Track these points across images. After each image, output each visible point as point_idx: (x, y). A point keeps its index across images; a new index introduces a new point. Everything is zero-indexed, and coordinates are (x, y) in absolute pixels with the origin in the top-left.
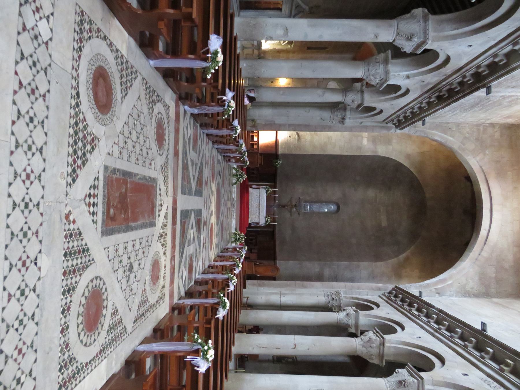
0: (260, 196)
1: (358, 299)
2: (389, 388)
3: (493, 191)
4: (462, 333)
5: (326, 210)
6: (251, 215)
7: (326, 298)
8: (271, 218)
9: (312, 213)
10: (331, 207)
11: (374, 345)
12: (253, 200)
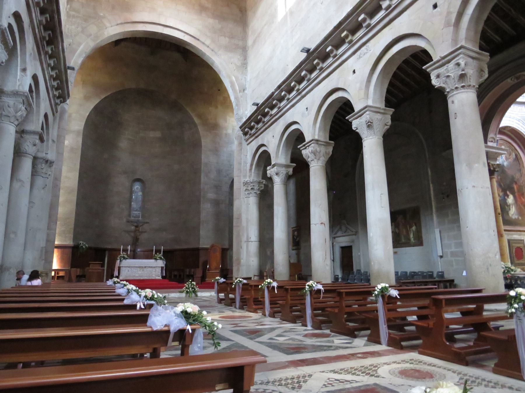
0: (129, 267)
1: (251, 165)
2: (373, 136)
4: (307, 70)
6: (153, 277)
7: (251, 195)
8: (156, 253)
9: (143, 208)
11: (318, 149)
12: (134, 274)
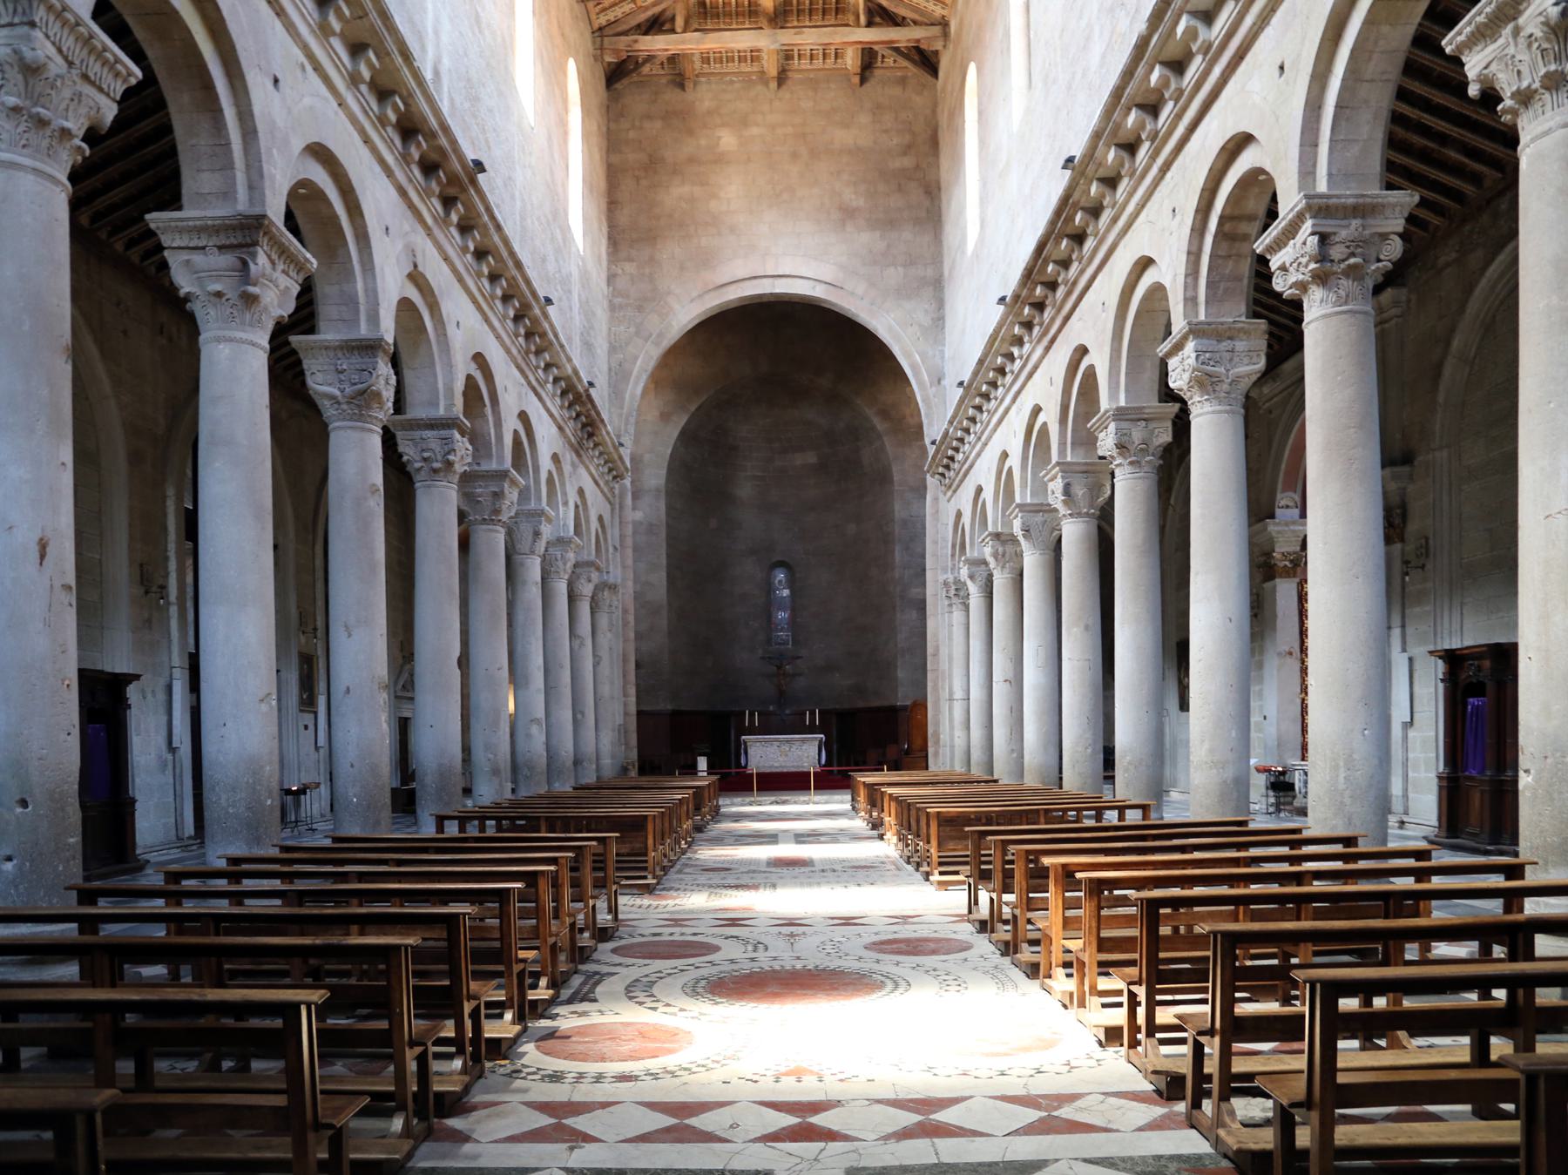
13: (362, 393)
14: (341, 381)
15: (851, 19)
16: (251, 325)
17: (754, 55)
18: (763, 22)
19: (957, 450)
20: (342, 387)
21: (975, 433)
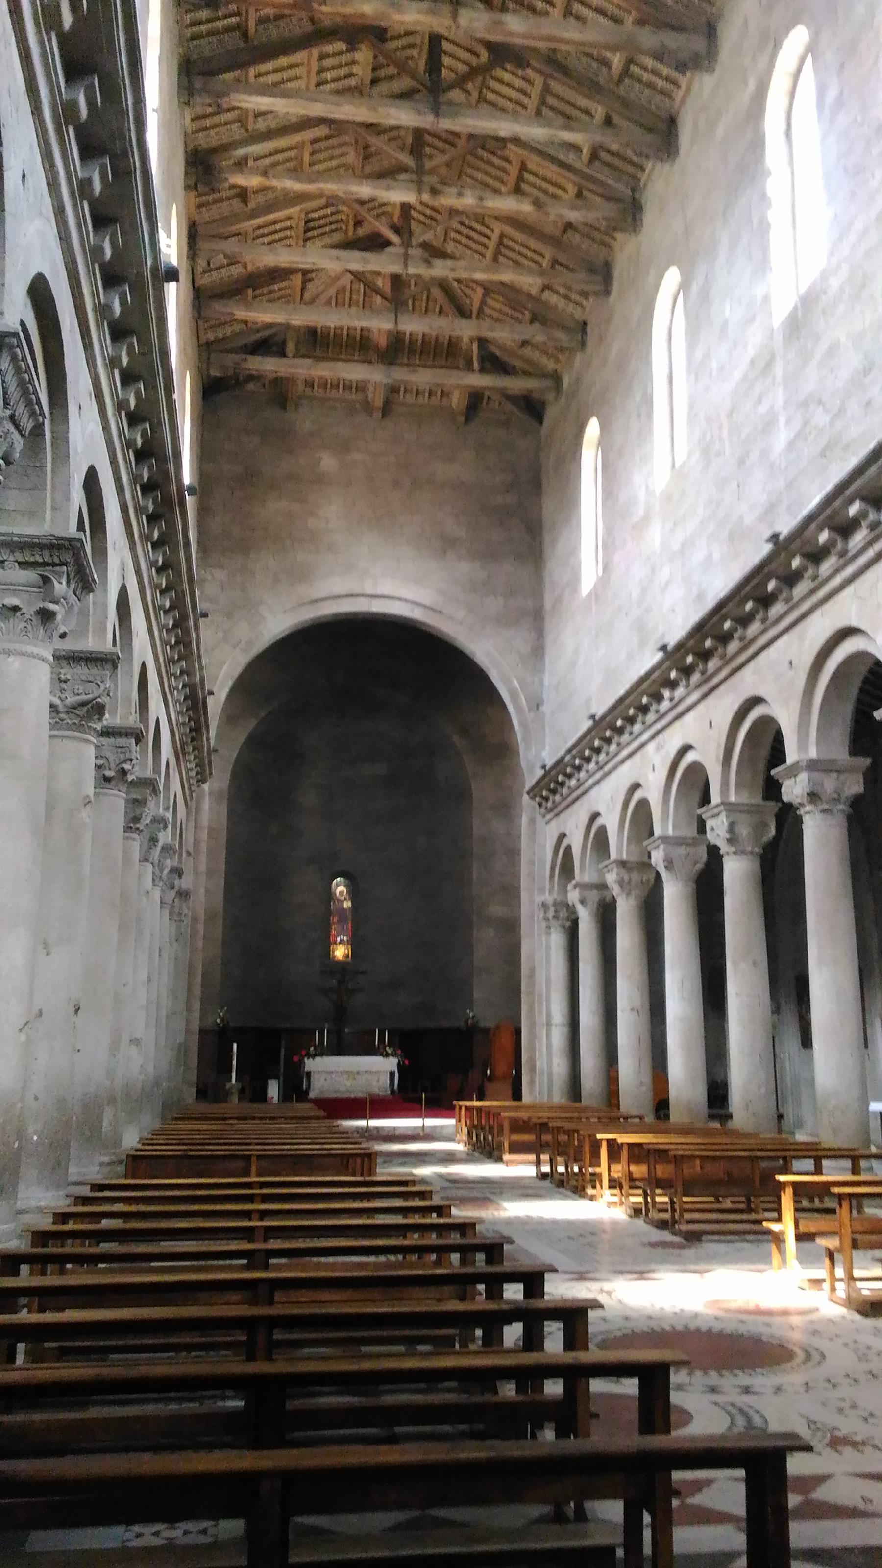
1: (553, 868)
3: (338, 589)
5: (347, 904)
10: (341, 893)
13: (84, 704)
14: (62, 690)
15: (461, 363)
16: (43, 641)
17: (361, 387)
18: (374, 357)
19: (570, 776)
20: (63, 696)
21: (597, 763)
